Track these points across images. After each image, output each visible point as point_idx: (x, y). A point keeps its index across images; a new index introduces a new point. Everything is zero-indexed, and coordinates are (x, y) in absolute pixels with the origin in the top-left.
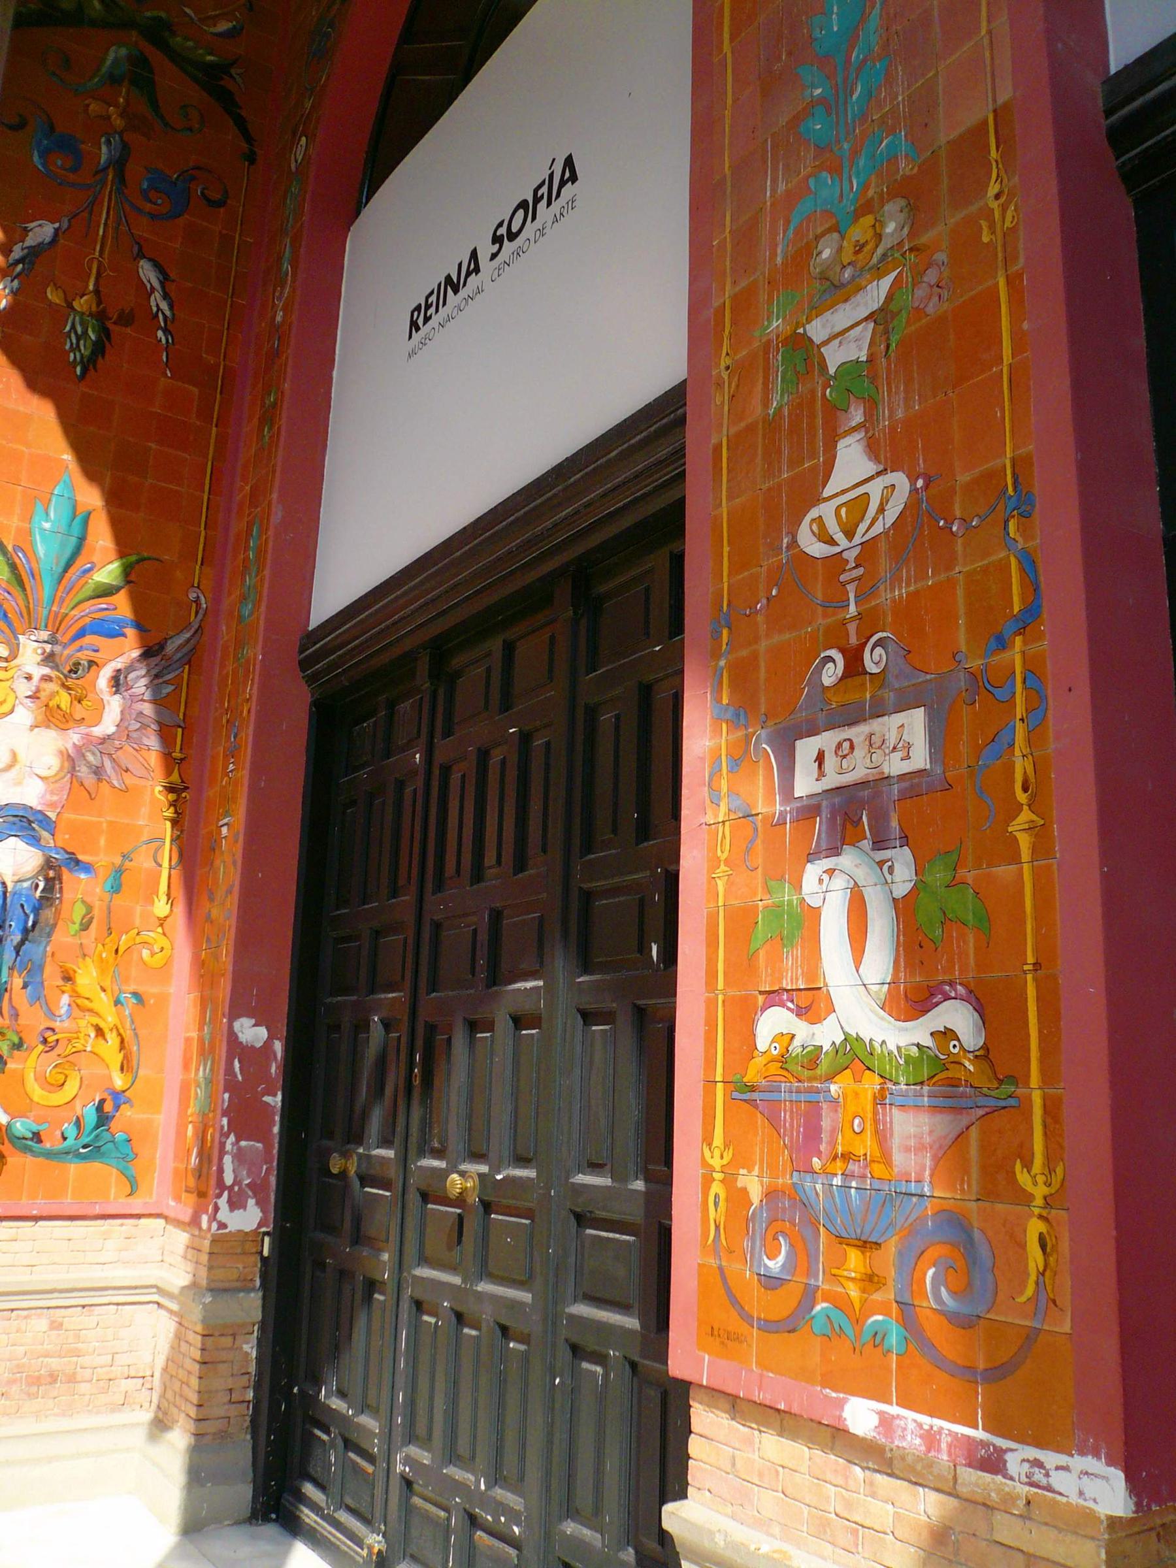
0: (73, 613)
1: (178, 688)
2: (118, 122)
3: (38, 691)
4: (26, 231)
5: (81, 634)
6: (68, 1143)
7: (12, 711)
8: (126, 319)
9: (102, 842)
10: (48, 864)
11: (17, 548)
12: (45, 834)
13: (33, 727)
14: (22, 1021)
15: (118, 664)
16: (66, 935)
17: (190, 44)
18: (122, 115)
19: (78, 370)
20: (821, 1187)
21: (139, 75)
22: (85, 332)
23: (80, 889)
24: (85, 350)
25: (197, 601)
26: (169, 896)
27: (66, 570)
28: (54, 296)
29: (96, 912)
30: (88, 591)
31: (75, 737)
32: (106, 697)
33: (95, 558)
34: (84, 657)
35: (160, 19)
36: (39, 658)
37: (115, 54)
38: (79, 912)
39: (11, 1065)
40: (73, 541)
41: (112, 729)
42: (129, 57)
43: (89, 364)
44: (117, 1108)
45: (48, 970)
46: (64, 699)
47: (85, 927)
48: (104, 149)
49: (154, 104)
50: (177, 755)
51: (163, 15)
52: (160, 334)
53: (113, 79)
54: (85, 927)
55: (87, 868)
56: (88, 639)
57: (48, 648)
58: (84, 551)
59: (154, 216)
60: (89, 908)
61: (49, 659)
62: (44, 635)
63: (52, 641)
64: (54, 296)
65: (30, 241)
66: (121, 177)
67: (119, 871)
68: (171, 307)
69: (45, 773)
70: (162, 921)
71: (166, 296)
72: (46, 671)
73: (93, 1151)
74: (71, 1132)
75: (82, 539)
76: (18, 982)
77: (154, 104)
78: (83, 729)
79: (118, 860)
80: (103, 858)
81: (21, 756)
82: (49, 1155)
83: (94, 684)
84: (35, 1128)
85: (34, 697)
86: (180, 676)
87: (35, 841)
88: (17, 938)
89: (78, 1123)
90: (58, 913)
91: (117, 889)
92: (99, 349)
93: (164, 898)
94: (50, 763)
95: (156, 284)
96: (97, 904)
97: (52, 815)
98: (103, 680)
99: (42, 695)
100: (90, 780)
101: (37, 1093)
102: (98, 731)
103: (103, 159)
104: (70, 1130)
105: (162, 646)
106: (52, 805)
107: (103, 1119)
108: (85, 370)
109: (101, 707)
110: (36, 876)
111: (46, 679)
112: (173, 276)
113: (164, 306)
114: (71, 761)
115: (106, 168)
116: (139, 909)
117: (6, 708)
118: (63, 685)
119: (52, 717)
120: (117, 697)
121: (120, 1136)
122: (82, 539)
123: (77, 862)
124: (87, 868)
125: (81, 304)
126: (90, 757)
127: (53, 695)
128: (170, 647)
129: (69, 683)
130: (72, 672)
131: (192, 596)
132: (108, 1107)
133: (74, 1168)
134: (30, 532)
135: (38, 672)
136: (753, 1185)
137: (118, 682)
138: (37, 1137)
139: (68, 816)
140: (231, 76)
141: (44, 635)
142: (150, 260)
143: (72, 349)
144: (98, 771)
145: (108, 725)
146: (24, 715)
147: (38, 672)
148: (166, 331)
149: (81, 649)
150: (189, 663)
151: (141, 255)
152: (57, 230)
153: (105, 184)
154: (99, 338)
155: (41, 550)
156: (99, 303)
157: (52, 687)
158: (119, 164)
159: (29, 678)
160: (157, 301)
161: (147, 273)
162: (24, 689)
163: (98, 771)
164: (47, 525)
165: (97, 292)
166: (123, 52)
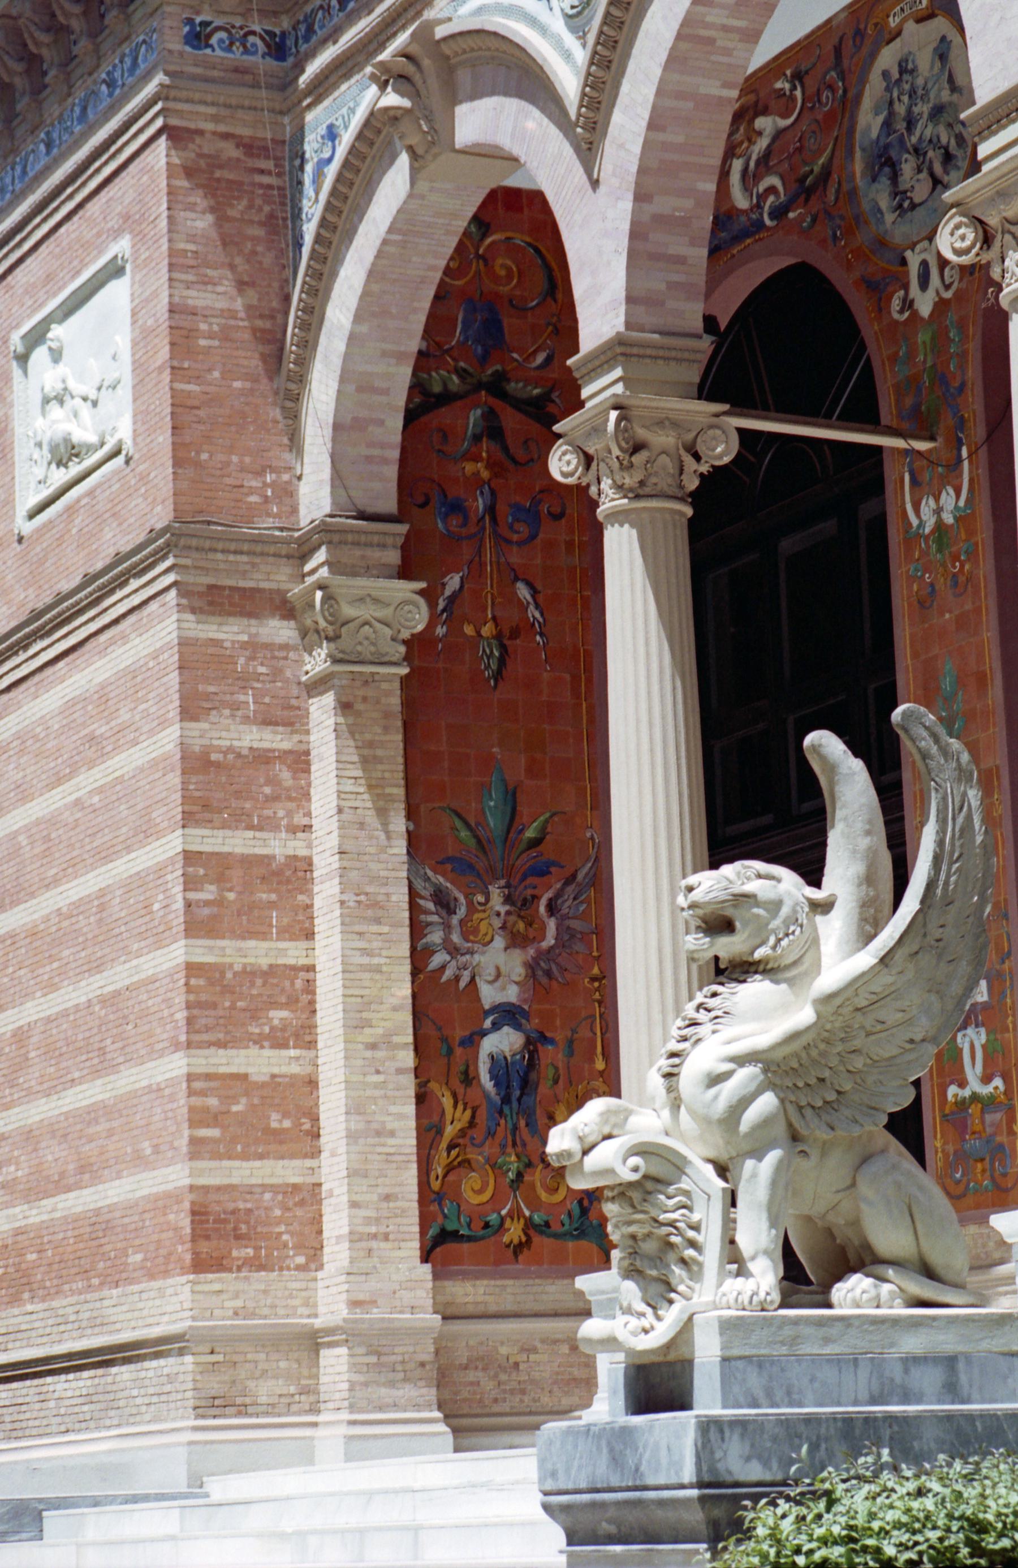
0: (519, 862)
1: (589, 904)
2: (485, 474)
3: (505, 923)
4: (444, 585)
5: (524, 878)
6: (567, 1227)
7: (492, 940)
8: (515, 633)
9: (558, 1023)
10: (529, 1042)
11: (478, 824)
12: (524, 1021)
13: (506, 949)
14: (529, 1148)
15: (549, 894)
16: (544, 1089)
17: (521, 385)
18: (487, 467)
19: (492, 682)
20: (973, 1144)
21: (492, 429)
22: (492, 652)
23: (550, 1055)
24: (494, 666)
25: (592, 838)
26: (603, 1054)
27: (508, 832)
28: (469, 630)
29: (561, 1072)
30: (523, 846)
31: (531, 951)
32: (546, 919)
33: (525, 820)
34: (529, 892)
35: (497, 371)
36: (502, 900)
37: (475, 415)
38: (551, 1072)
39: (526, 1178)
40: (509, 809)
41: (553, 942)
42: (483, 415)
43: (498, 675)
44: (591, 1203)
45: (538, 1112)
46: (521, 926)
47: (556, 1082)
48: (480, 501)
49: (506, 449)
50: (595, 954)
51: (499, 367)
52: (538, 638)
53: (477, 438)
54: (556, 1082)
55: (552, 1041)
56: (530, 880)
57: (506, 891)
58: (517, 818)
59: (520, 543)
60: (556, 1069)
61: (508, 900)
62: (502, 882)
63: (508, 886)
64: (469, 630)
65: (448, 592)
66: (494, 520)
67: (571, 1042)
68: (542, 615)
69: (517, 979)
70: (601, 1073)
71: (537, 606)
72: (507, 908)
73: (581, 1233)
74: (567, 1221)
75: (514, 810)
76: (522, 1123)
77: (506, 449)
78: (535, 945)
79: (569, 1033)
80: (559, 1036)
81: (503, 969)
82: (556, 1236)
83: (537, 910)
84: (545, 1218)
85: (503, 927)
86: (589, 896)
87: (518, 1027)
88: (518, 1093)
89: (570, 1215)
90: (539, 1072)
91: (571, 1054)
92: (502, 662)
93: (601, 1057)
94: (518, 971)
95: (529, 597)
96: (560, 1065)
97: (526, 1007)
98: (542, 909)
99: (508, 925)
100: (544, 980)
101: (544, 1196)
102: (545, 945)
103: (481, 507)
104: (564, 1217)
105: (574, 876)
106: (525, 1001)
107: (584, 1211)
108: (496, 681)
109: (543, 928)
110: (522, 1052)
111: (508, 913)
112: (539, 588)
113: (537, 615)
114: (531, 967)
115: (483, 517)
116: (586, 1066)
117: (488, 938)
118: (519, 916)
119: (516, 941)
120: (553, 919)
121: (595, 1222)
122: (514, 810)
123: (545, 1038)
124: (552, 1041)
125: (487, 630)
126: (542, 964)
127: (515, 924)
128: (580, 876)
129: (522, 913)
130: (521, 905)
131: (588, 835)
132: (586, 1203)
133: (571, 1244)
134: (484, 813)
135: (503, 909)
136: (951, 1148)
137: (552, 909)
138: (547, 1224)
139: (535, 1006)
140: (553, 401)
141: (502, 882)
142: (523, 580)
143: (486, 668)
144: (548, 973)
145: (550, 941)
146: (499, 942)
147: (503, 909)
148: (541, 634)
149: (526, 888)
150: (593, 885)
151: (517, 579)
152: (462, 578)
153: (484, 529)
154: (501, 655)
155: (492, 824)
156: (496, 626)
157: (512, 918)
158: (491, 509)
159: (498, 914)
160: (533, 613)
161: (523, 592)
162: (497, 923)
163: (548, 973)
164: (492, 804)
165: (494, 618)
166: (479, 412)
